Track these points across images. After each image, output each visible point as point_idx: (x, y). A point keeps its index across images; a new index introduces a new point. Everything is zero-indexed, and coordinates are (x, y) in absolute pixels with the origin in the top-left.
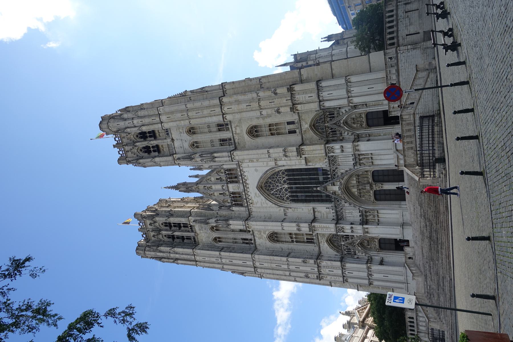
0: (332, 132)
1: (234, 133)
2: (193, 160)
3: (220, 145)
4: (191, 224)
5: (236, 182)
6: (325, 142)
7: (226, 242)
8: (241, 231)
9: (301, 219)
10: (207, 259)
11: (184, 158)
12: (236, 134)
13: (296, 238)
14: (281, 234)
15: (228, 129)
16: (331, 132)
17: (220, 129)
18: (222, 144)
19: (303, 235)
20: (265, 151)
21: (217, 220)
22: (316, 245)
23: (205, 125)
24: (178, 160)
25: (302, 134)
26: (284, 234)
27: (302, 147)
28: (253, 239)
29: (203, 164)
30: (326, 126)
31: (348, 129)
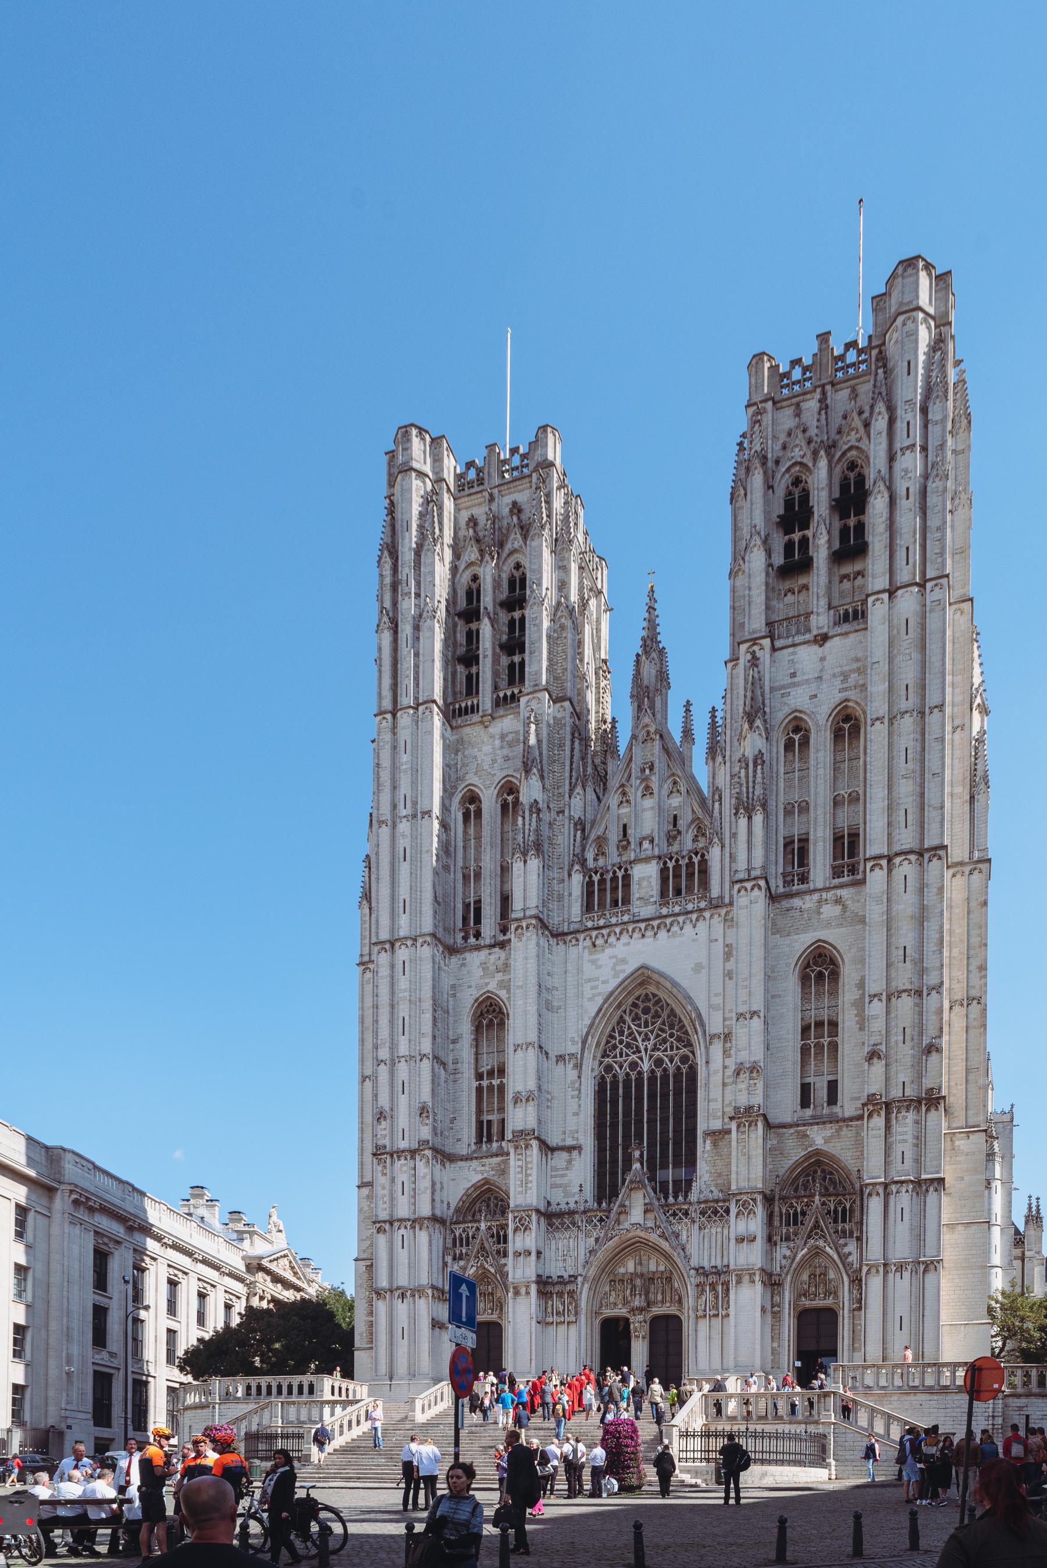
0: (795, 1214)
1: (824, 895)
2: (746, 726)
3: (788, 840)
4: (523, 700)
5: (663, 893)
6: (768, 1192)
7: (466, 840)
8: (505, 900)
9: (548, 1107)
10: (405, 758)
11: (755, 684)
12: (820, 901)
13: (491, 1087)
14: (501, 1040)
15: (837, 872)
16: (796, 1210)
17: (839, 842)
18: (789, 848)
19: (502, 1109)
20: (758, 1005)
21: (539, 811)
22: (473, 1147)
23: (862, 784)
24: (749, 656)
25: (798, 1125)
26: (501, 1051)
27: (760, 1125)
28: (482, 942)
29: (728, 764)
30: (813, 1196)
31: (798, 1259)
